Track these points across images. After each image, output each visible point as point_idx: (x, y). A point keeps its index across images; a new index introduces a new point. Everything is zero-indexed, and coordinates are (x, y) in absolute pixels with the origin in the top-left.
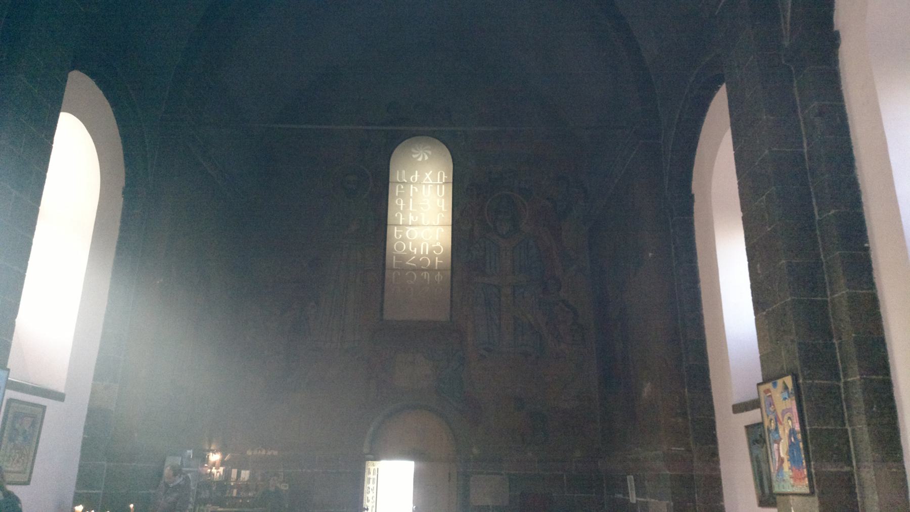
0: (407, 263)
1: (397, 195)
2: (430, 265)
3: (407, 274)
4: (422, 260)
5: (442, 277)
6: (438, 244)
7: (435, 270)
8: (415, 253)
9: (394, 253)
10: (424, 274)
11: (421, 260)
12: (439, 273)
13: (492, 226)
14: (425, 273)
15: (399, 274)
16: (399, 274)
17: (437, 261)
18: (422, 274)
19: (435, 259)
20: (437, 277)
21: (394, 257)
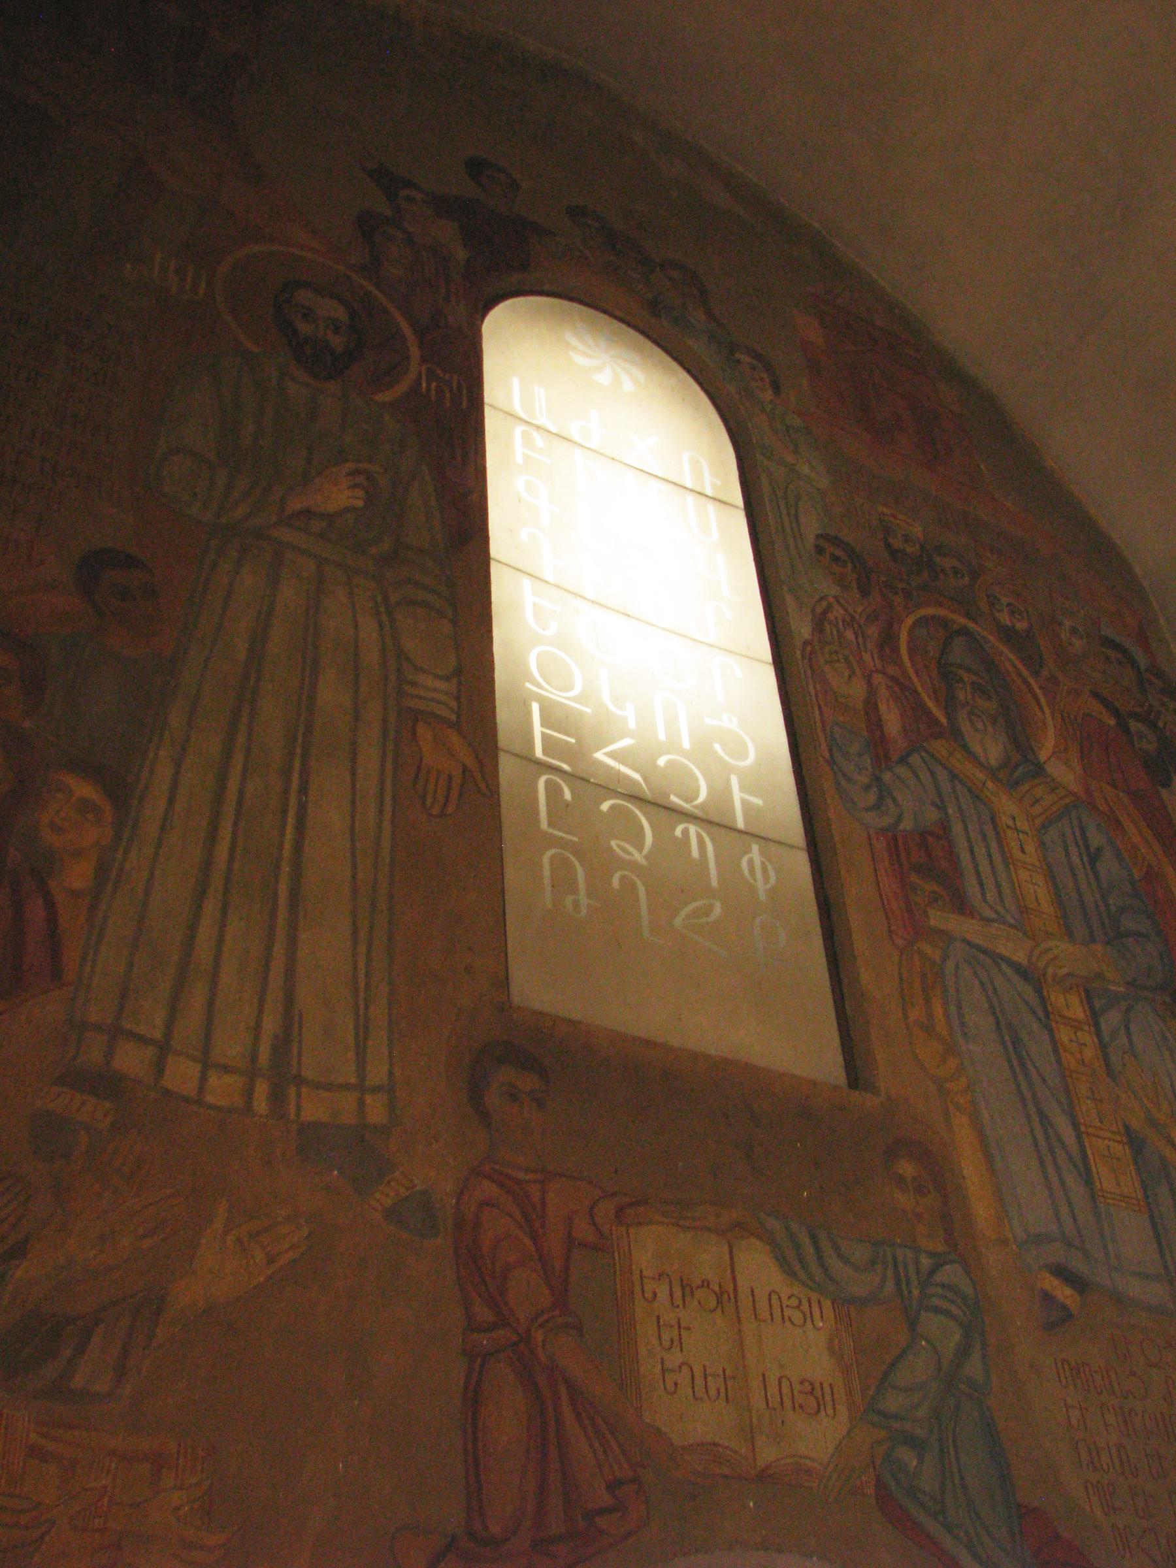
0: (599, 755)
1: (519, 459)
2: (704, 802)
3: (605, 806)
4: (670, 763)
5: (773, 880)
6: (731, 723)
7: (740, 832)
8: (632, 724)
9: (528, 685)
10: (686, 832)
11: (662, 762)
12: (755, 848)
13: (944, 721)
14: (693, 829)
15: (568, 795)
16: (568, 795)
17: (737, 796)
18: (678, 832)
19: (728, 780)
20: (751, 863)
21: (535, 708)
